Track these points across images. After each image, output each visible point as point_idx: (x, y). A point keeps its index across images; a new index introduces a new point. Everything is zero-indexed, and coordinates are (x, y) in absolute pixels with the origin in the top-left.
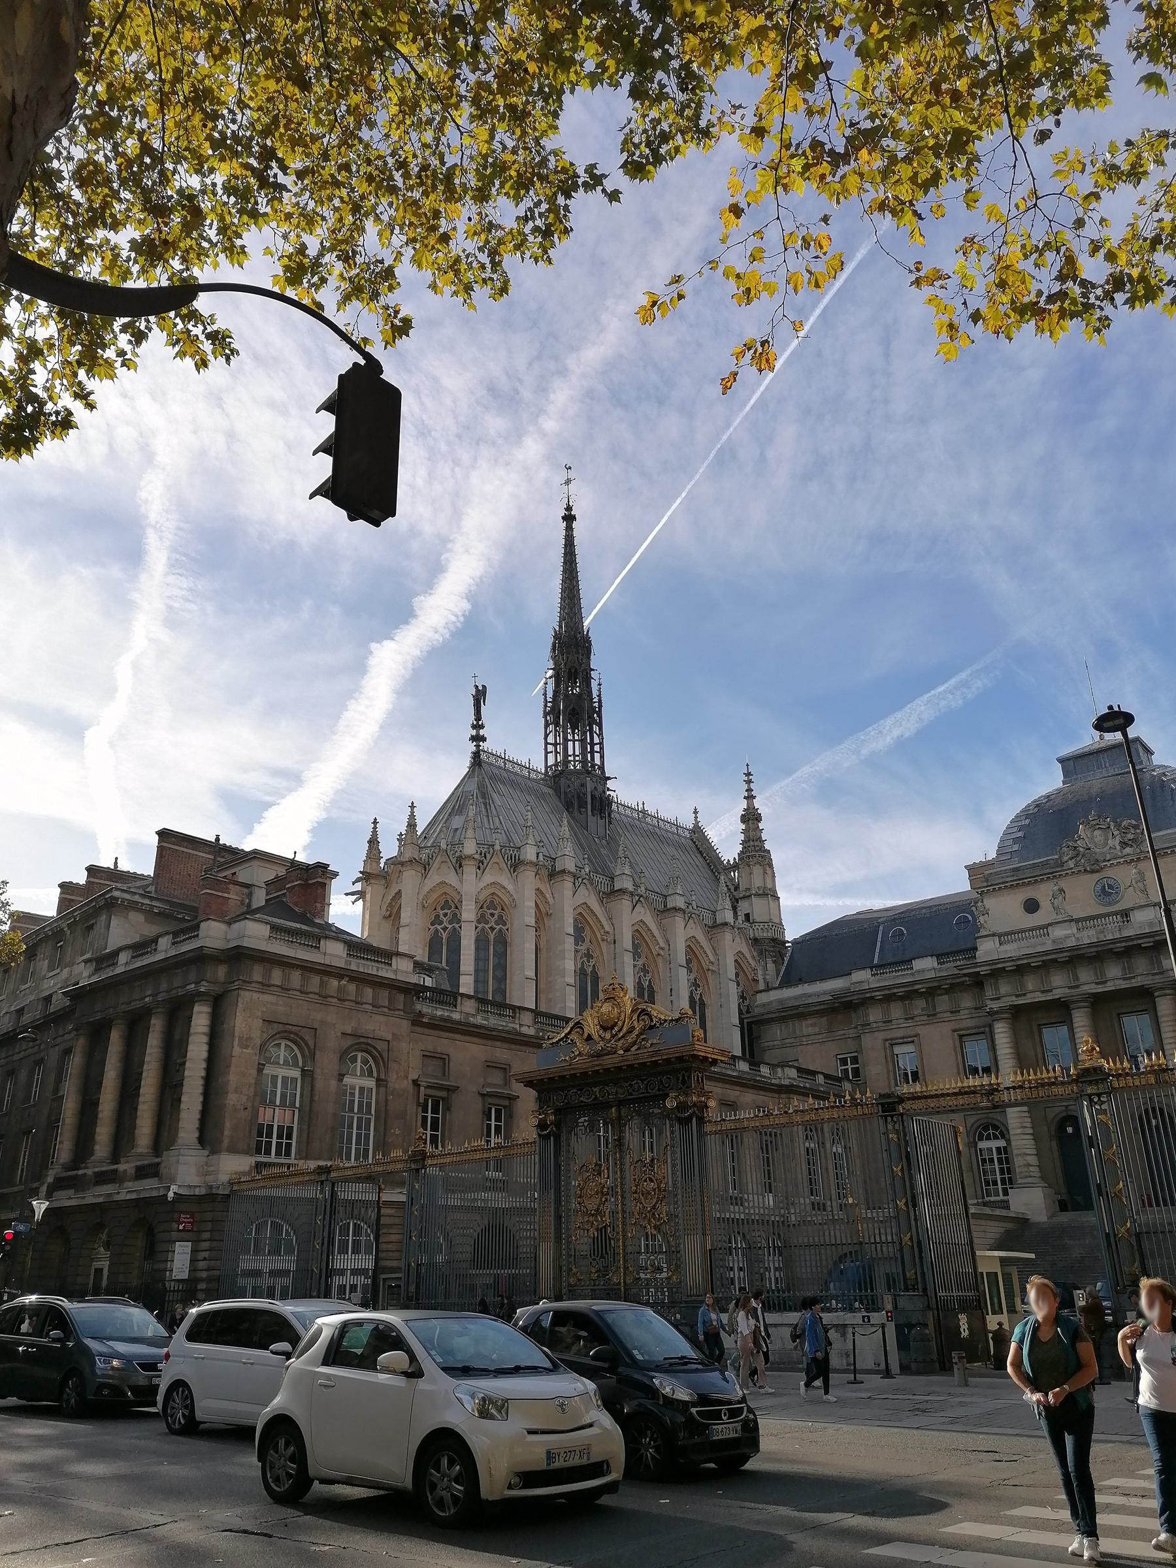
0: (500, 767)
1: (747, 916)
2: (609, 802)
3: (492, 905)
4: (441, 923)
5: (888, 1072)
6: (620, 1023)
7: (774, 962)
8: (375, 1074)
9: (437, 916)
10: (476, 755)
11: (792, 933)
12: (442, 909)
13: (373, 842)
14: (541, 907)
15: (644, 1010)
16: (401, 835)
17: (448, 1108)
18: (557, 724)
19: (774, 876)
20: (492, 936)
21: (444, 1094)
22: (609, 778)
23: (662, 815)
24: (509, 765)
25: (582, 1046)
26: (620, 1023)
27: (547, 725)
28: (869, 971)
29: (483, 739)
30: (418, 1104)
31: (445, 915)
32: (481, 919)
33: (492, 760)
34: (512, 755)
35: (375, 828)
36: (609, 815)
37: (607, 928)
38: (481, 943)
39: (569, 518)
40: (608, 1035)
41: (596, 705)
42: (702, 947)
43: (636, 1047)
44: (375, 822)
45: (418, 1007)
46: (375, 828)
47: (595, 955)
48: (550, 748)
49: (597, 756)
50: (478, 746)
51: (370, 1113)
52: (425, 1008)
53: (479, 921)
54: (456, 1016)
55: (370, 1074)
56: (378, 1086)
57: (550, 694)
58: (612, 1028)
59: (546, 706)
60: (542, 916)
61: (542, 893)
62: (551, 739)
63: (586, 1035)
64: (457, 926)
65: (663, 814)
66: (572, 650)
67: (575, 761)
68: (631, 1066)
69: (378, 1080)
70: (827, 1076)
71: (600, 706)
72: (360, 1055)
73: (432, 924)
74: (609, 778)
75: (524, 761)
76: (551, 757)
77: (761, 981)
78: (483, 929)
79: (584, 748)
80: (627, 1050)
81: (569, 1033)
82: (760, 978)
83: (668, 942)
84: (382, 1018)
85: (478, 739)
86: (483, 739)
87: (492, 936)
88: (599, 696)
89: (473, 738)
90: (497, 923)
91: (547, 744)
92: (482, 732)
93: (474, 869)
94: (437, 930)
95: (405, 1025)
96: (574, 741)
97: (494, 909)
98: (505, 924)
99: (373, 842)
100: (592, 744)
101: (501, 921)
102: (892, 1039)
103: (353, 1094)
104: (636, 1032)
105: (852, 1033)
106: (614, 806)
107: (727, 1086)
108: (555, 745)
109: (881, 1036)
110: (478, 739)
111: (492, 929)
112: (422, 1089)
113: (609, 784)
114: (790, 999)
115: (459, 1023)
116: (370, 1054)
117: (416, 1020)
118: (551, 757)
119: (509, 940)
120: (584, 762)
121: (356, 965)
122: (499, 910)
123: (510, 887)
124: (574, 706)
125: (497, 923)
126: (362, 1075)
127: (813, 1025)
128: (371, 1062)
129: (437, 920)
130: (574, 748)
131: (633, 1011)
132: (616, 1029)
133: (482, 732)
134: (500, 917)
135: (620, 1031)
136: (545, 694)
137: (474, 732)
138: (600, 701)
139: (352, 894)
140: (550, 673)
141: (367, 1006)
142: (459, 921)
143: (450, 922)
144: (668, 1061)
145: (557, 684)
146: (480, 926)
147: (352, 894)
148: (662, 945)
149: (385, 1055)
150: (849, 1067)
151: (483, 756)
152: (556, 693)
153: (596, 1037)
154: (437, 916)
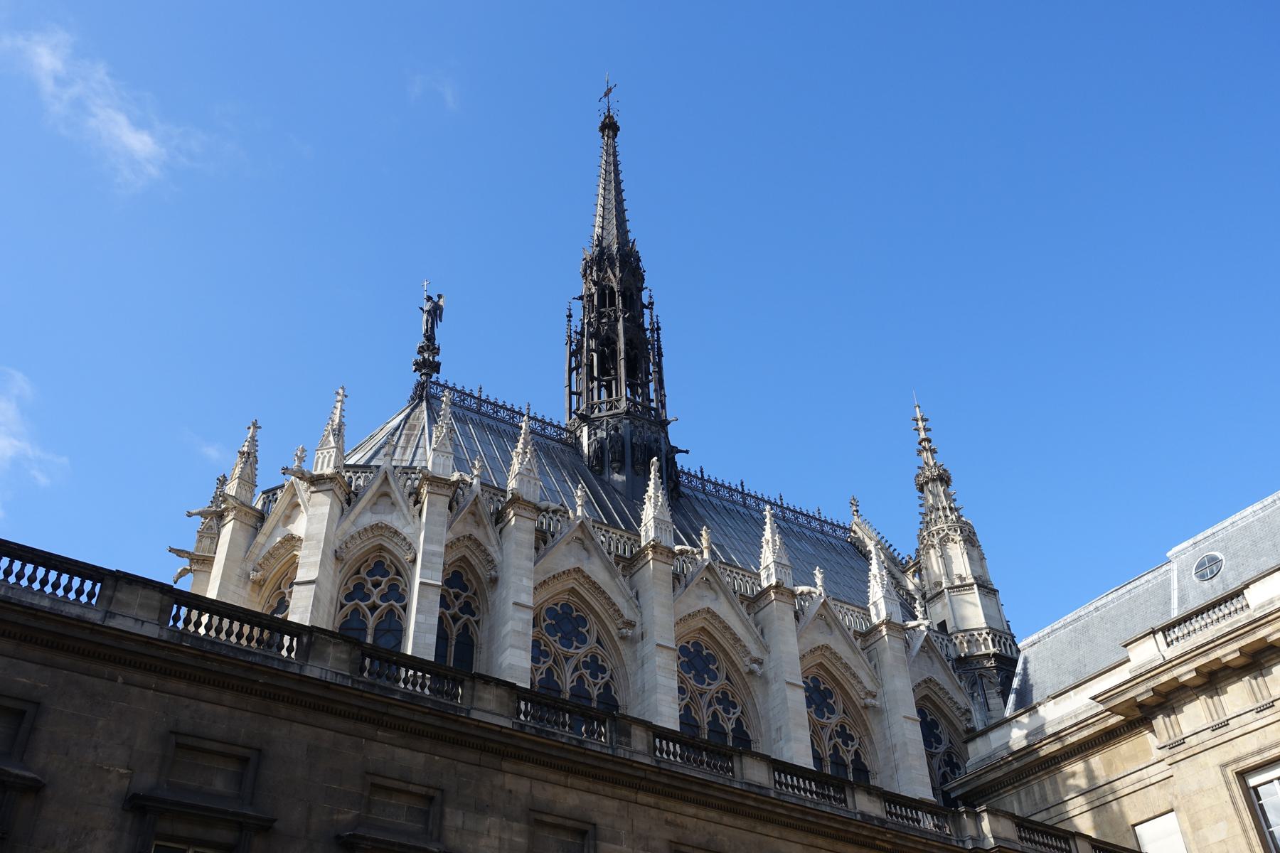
5: (1245, 831)
20: (371, 621)
28: (1160, 636)
37: (628, 614)
39: (610, 127)
42: (847, 667)
47: (608, 666)
83: (766, 649)
85: (428, 366)
87: (371, 621)
90: (384, 598)
102: (1236, 761)
109: (1212, 759)
110: (428, 366)
111: (373, 608)
123: (406, 531)
125: (384, 598)
148: (755, 652)
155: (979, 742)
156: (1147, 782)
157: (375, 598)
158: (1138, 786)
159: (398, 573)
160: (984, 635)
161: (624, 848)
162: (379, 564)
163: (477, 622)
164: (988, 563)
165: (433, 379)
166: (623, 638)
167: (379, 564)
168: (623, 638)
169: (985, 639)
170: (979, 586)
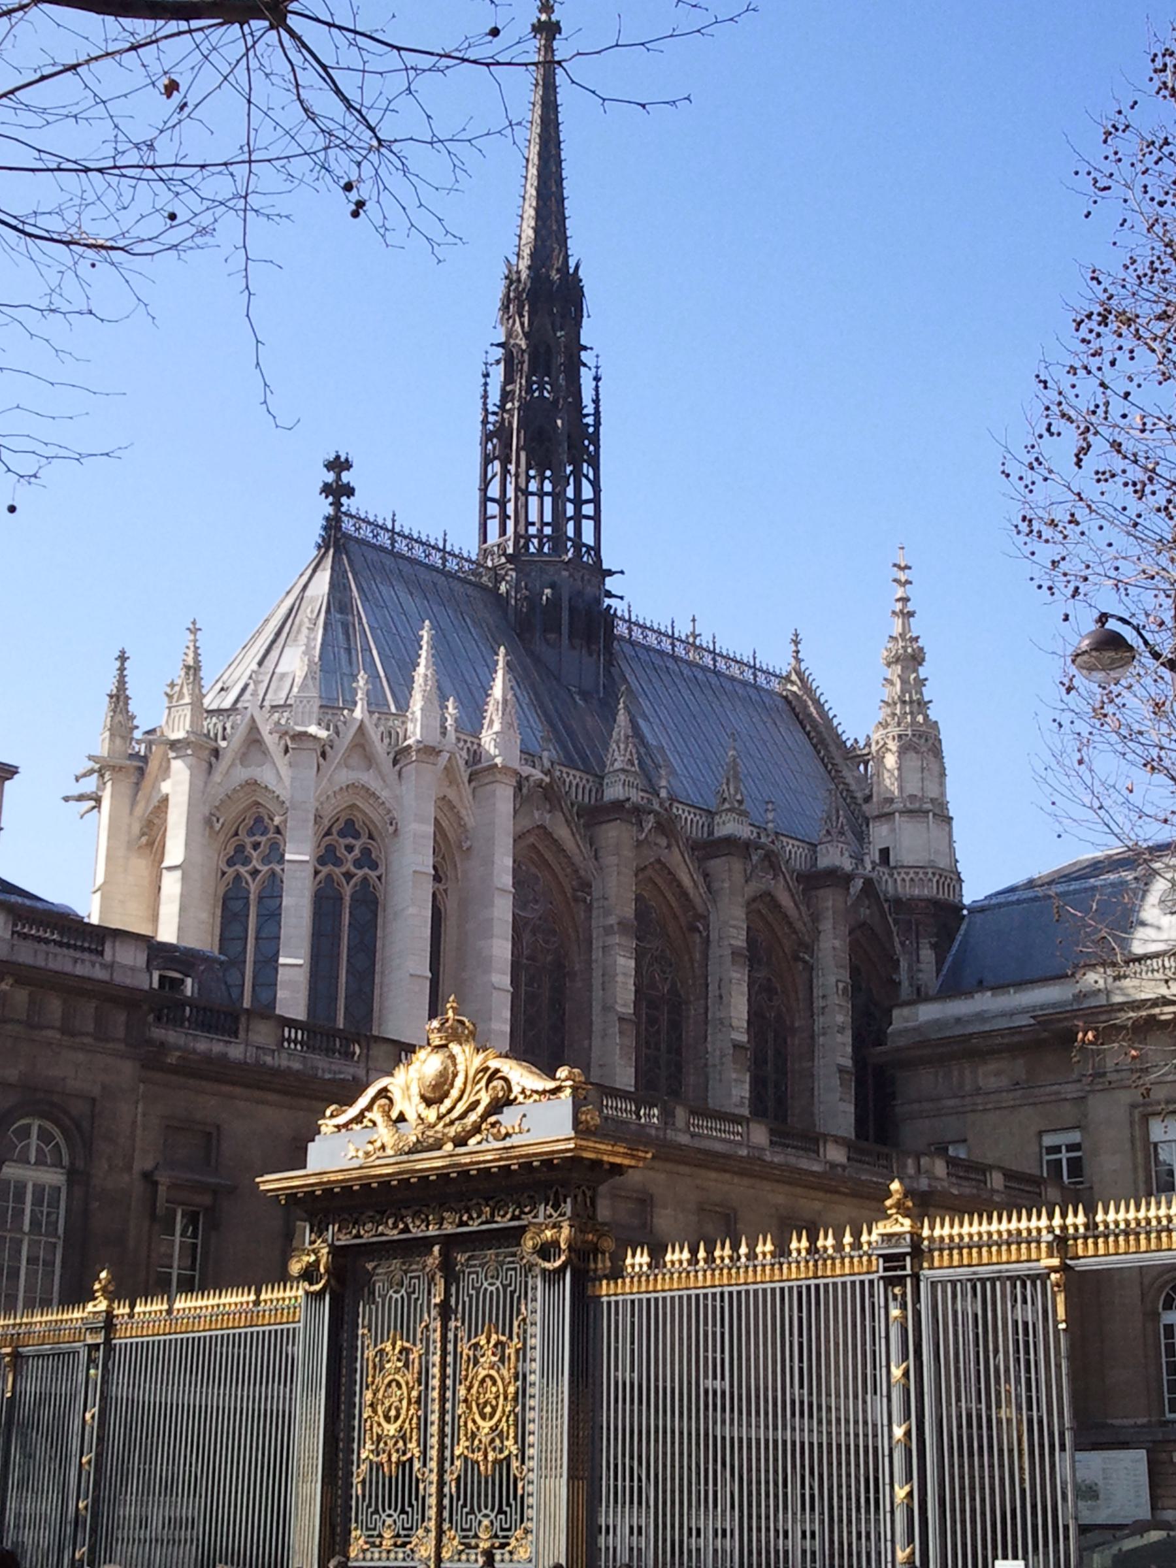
0: (381, 548)
1: (885, 853)
2: (609, 617)
3: (350, 829)
4: (247, 861)
5: (1135, 1168)
6: (454, 1093)
7: (934, 946)
8: (66, 1160)
9: (240, 849)
10: (333, 524)
11: (973, 892)
12: (251, 832)
13: (119, 698)
14: (451, 835)
15: (497, 1071)
16: (172, 685)
17: (214, 1225)
18: (505, 462)
19: (943, 774)
20: (347, 891)
21: (207, 1200)
22: (610, 573)
23: (723, 646)
24: (401, 546)
25: (384, 1134)
26: (454, 1093)
27: (487, 460)
29: (349, 491)
30: (153, 1217)
31: (256, 846)
32: (327, 857)
33: (366, 533)
34: (408, 523)
35: (122, 669)
36: (608, 648)
38: (325, 902)
40: (431, 1115)
41: (590, 420)
43: (478, 1137)
44: (122, 658)
45: (158, 1033)
46: (122, 669)
48: (493, 509)
49: (588, 526)
50: (337, 504)
51: (56, 1235)
52: (172, 1036)
53: (321, 860)
54: (236, 1052)
55: (58, 1164)
56: (70, 1182)
57: (495, 397)
58: (441, 1102)
59: (485, 422)
60: (451, 852)
61: (452, 807)
62: (494, 491)
63: (394, 1115)
64: (278, 868)
65: (725, 645)
66: (548, 304)
67: (540, 535)
68: (464, 1174)
69: (74, 1176)
70: (1009, 1175)
71: (597, 424)
72: (36, 1124)
73: (230, 862)
74: (610, 573)
75: (435, 537)
76: (493, 526)
77: (905, 984)
78: (329, 876)
79: (558, 512)
80: (460, 1141)
81: (369, 1108)
82: (903, 975)
84: (81, 1057)
85: (338, 491)
86: (349, 491)
87: (347, 891)
88: (596, 401)
89: (327, 489)
90: (358, 864)
91: (485, 500)
92: (346, 477)
93: (314, 758)
94: (238, 877)
95: (128, 1069)
96: (541, 494)
97: (352, 841)
98: (374, 866)
99: (119, 698)
100: (578, 502)
101: (367, 860)
103: (20, 1197)
104: (480, 1109)
105: (1071, 1091)
106: (621, 629)
107: (799, 1190)
108: (502, 502)
110: (338, 491)
111: (348, 876)
112: (162, 1190)
113: (610, 583)
114: (958, 1020)
115: (242, 1065)
116: (57, 1122)
117: (152, 1059)
118: (493, 526)
119: (381, 899)
120: (558, 539)
121: (26, 954)
122: (364, 839)
123: (384, 794)
124: (545, 419)
125: (358, 864)
126: (40, 1162)
127: (997, 1074)
128: (59, 1138)
129: (238, 856)
130: (538, 510)
131: (477, 1072)
132: (448, 1103)
133: (346, 477)
134: (366, 852)
135: (450, 1111)
136: (485, 397)
137: (330, 477)
138: (597, 414)
139: (81, 798)
140: (499, 353)
141: (50, 1033)
142: (281, 859)
143: (266, 860)
144: (527, 1166)
145: (509, 379)
146: (325, 870)
147: (81, 798)
149: (85, 1124)
150: (1064, 1156)
151: (348, 525)
152: (505, 396)
153: (411, 1116)
154: (240, 849)
155: (906, 1011)
156: (1063, 1096)
157: (349, 866)
158: (1053, 1097)
159: (371, 837)
160: (930, 875)
161: (669, 1211)
162: (350, 823)
163: (445, 891)
164: (949, 781)
165: (343, 509)
166: (576, 900)
167: (350, 823)
168: (576, 900)
169: (930, 880)
170: (934, 815)
